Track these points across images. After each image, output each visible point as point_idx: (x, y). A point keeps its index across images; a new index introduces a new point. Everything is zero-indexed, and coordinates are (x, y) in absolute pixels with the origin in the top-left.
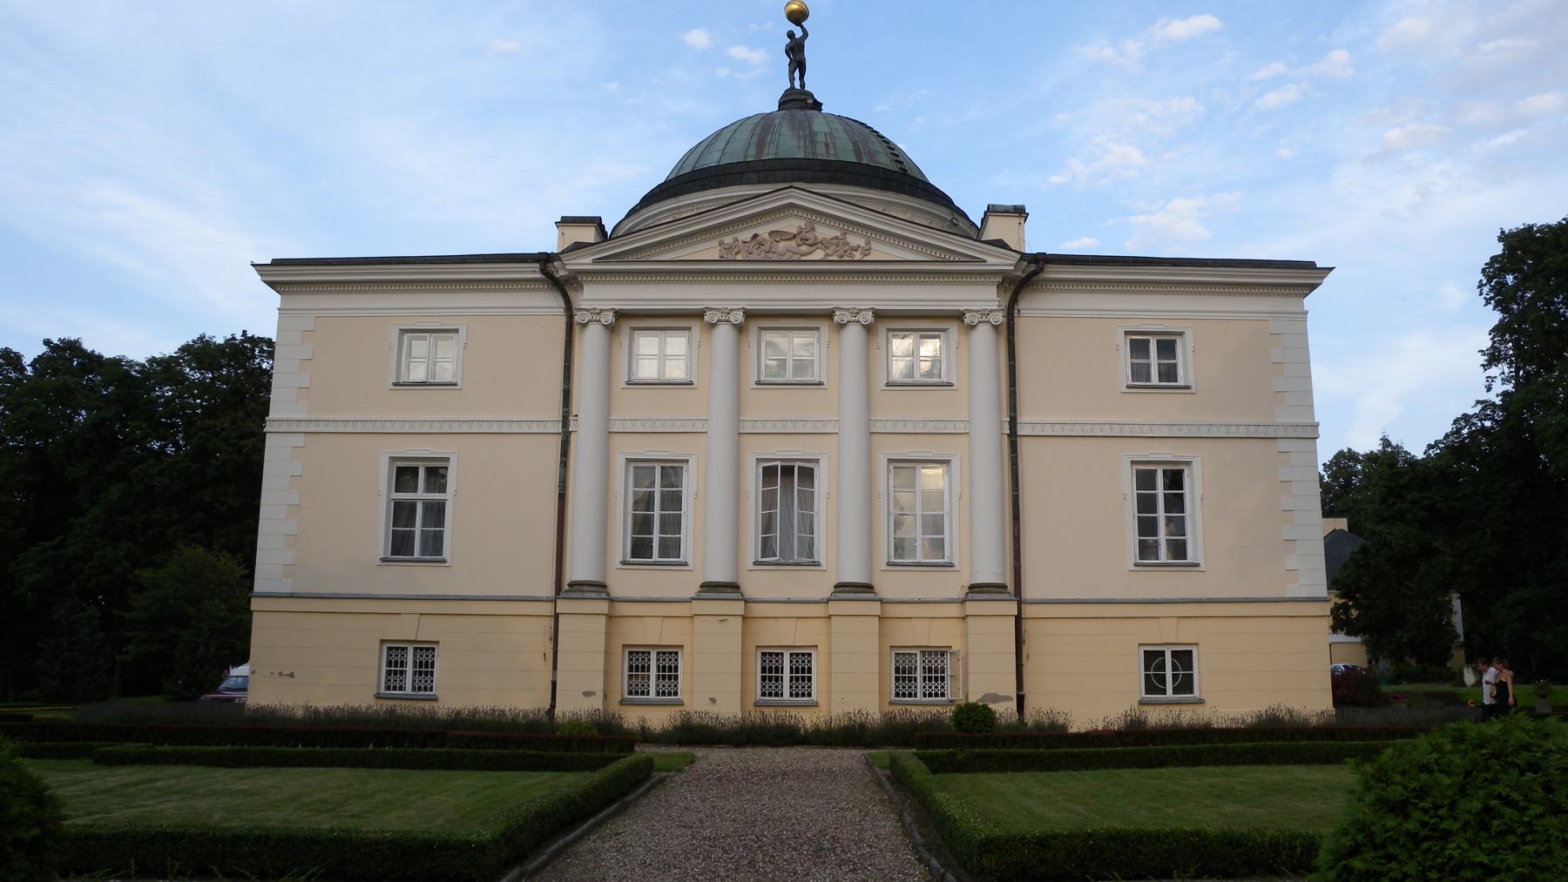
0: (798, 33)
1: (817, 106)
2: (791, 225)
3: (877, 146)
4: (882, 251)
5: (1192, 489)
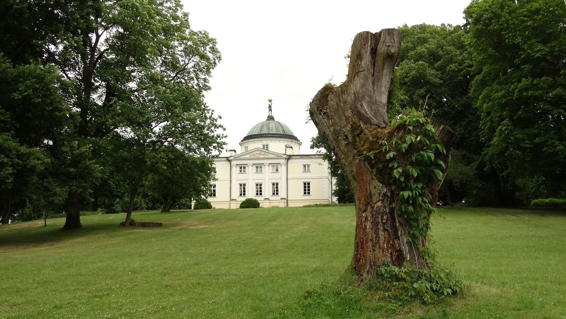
0: (270, 104)
1: (273, 118)
2: (258, 152)
3: (280, 129)
4: (270, 156)
5: (311, 185)
